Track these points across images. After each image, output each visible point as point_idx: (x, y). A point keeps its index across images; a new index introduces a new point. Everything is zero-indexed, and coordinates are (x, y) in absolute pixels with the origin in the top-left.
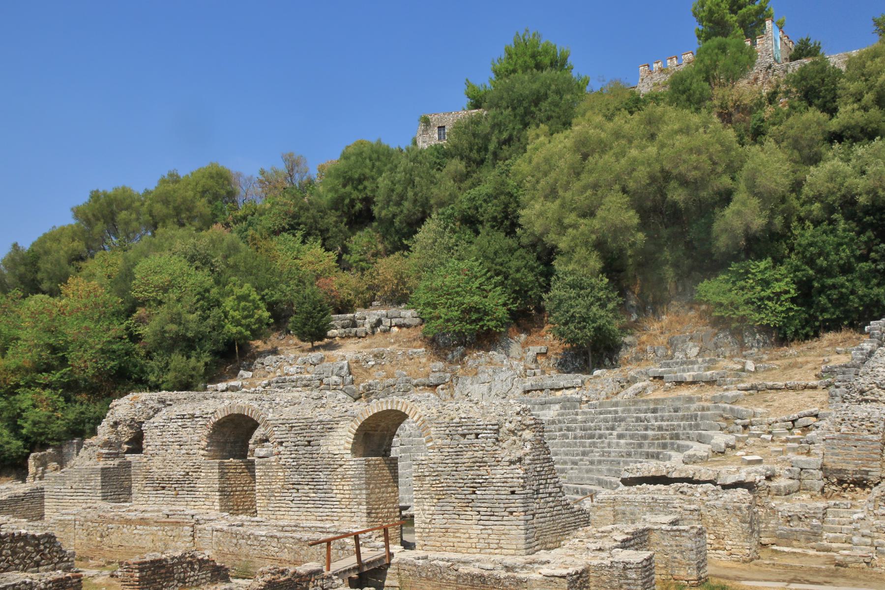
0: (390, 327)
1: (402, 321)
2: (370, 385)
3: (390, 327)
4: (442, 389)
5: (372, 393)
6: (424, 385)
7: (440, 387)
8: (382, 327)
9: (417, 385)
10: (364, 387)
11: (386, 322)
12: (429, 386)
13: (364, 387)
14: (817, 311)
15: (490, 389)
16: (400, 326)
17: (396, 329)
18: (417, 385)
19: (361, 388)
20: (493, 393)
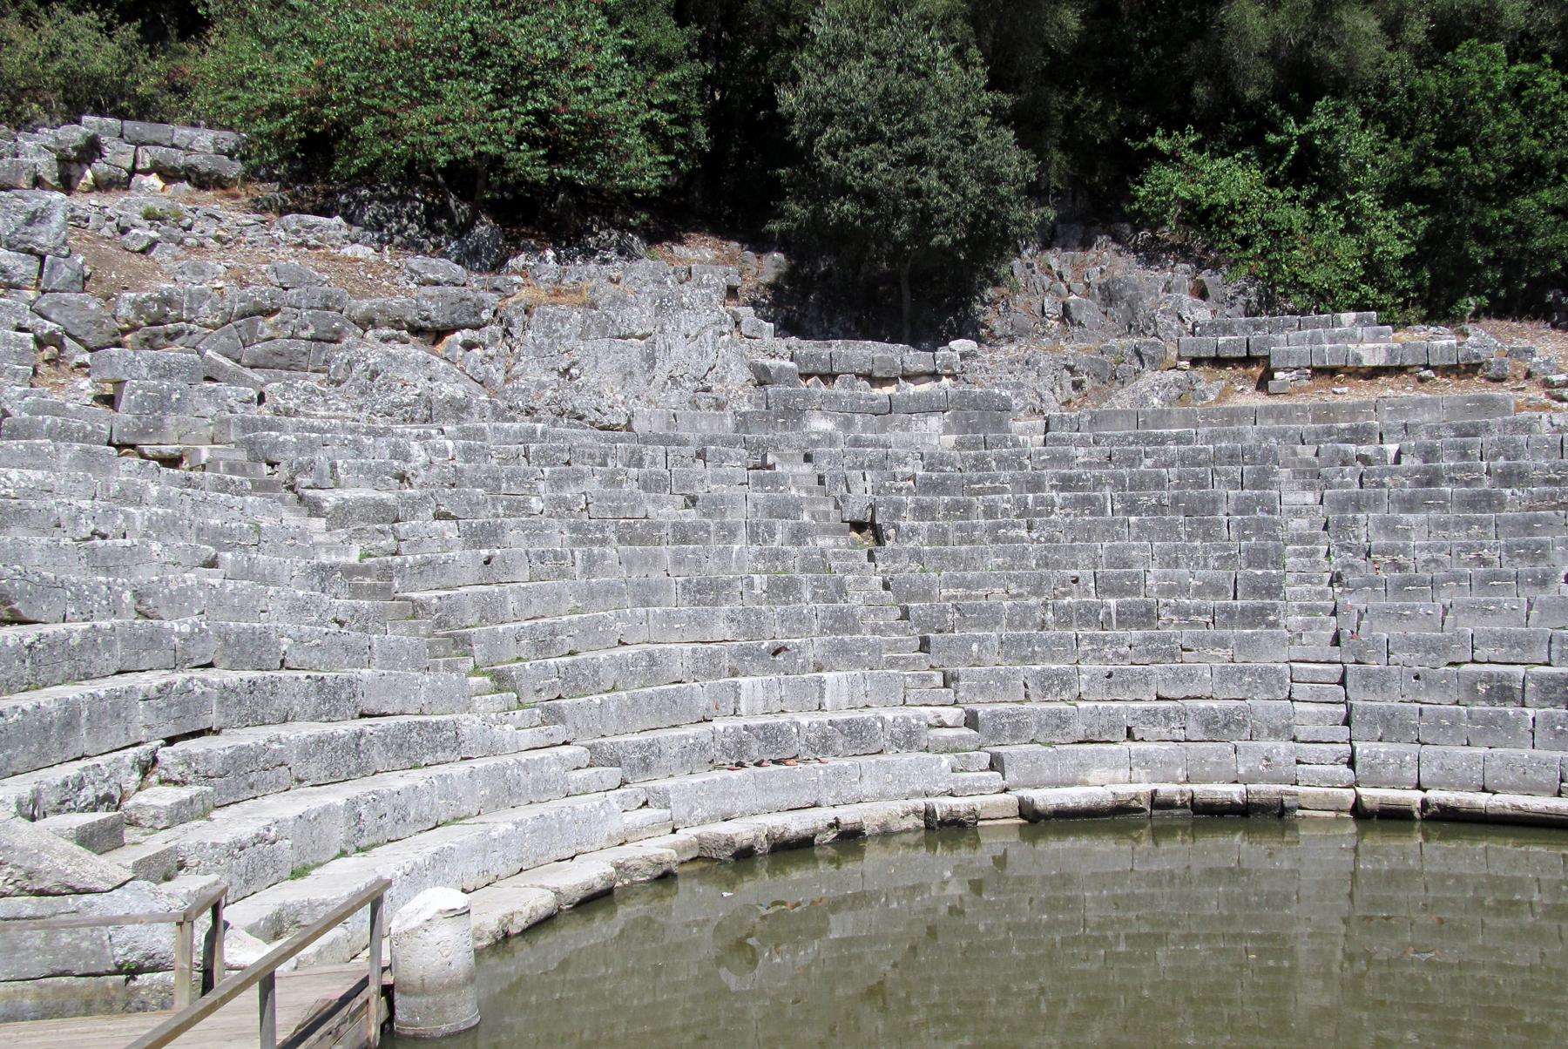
0: (133, 171)
1: (181, 159)
2: (167, 301)
3: (133, 171)
4: (469, 346)
5: (171, 337)
6: (396, 324)
7: (459, 336)
8: (100, 166)
9: (367, 323)
10: (139, 307)
11: (117, 155)
12: (416, 331)
13: (139, 307)
14: (1468, 263)
15: (650, 360)
16: (169, 175)
17: (154, 180)
18: (367, 323)
19: (125, 310)
20: (661, 375)
